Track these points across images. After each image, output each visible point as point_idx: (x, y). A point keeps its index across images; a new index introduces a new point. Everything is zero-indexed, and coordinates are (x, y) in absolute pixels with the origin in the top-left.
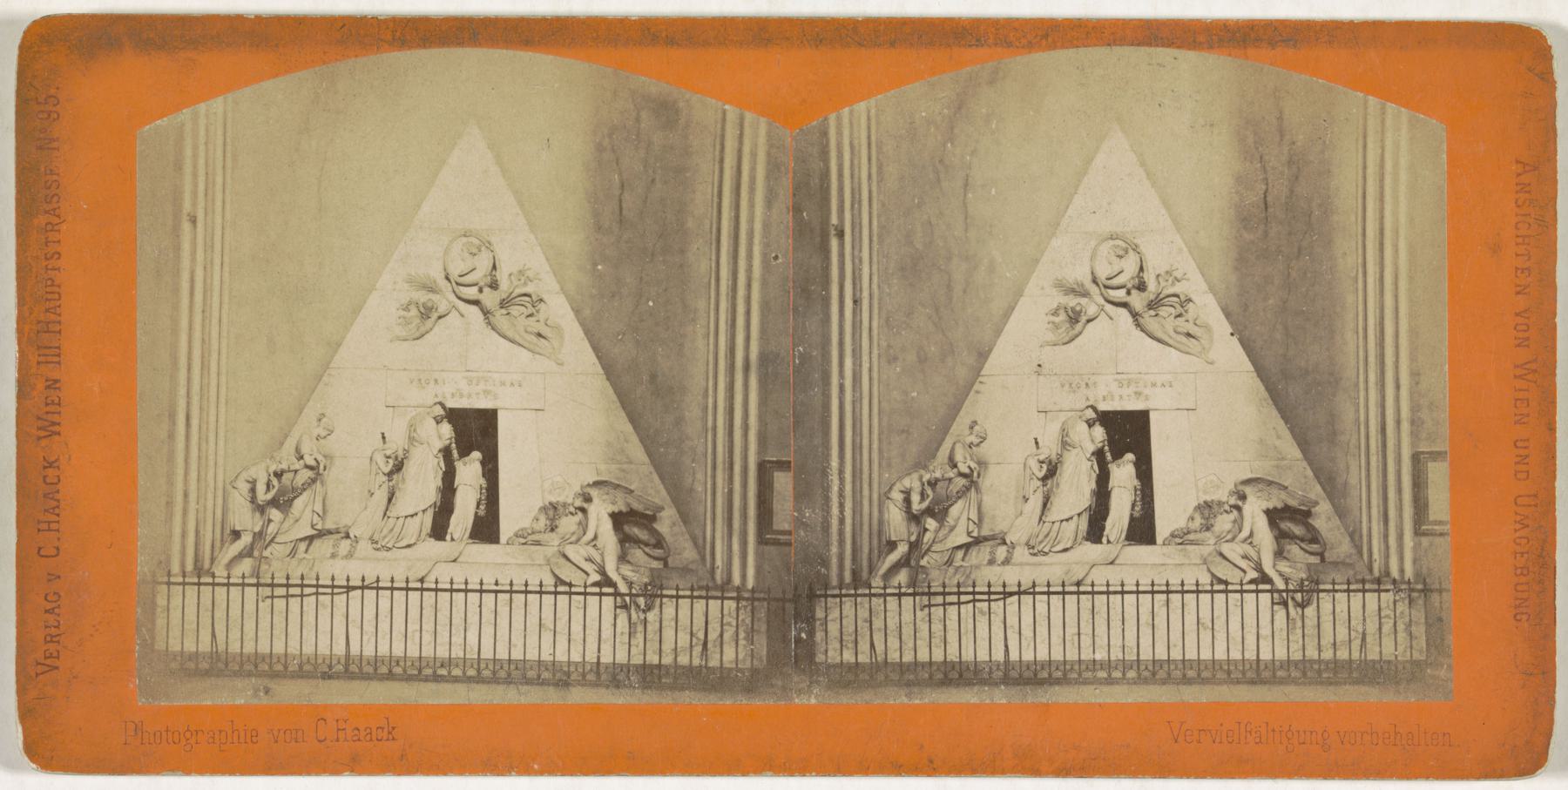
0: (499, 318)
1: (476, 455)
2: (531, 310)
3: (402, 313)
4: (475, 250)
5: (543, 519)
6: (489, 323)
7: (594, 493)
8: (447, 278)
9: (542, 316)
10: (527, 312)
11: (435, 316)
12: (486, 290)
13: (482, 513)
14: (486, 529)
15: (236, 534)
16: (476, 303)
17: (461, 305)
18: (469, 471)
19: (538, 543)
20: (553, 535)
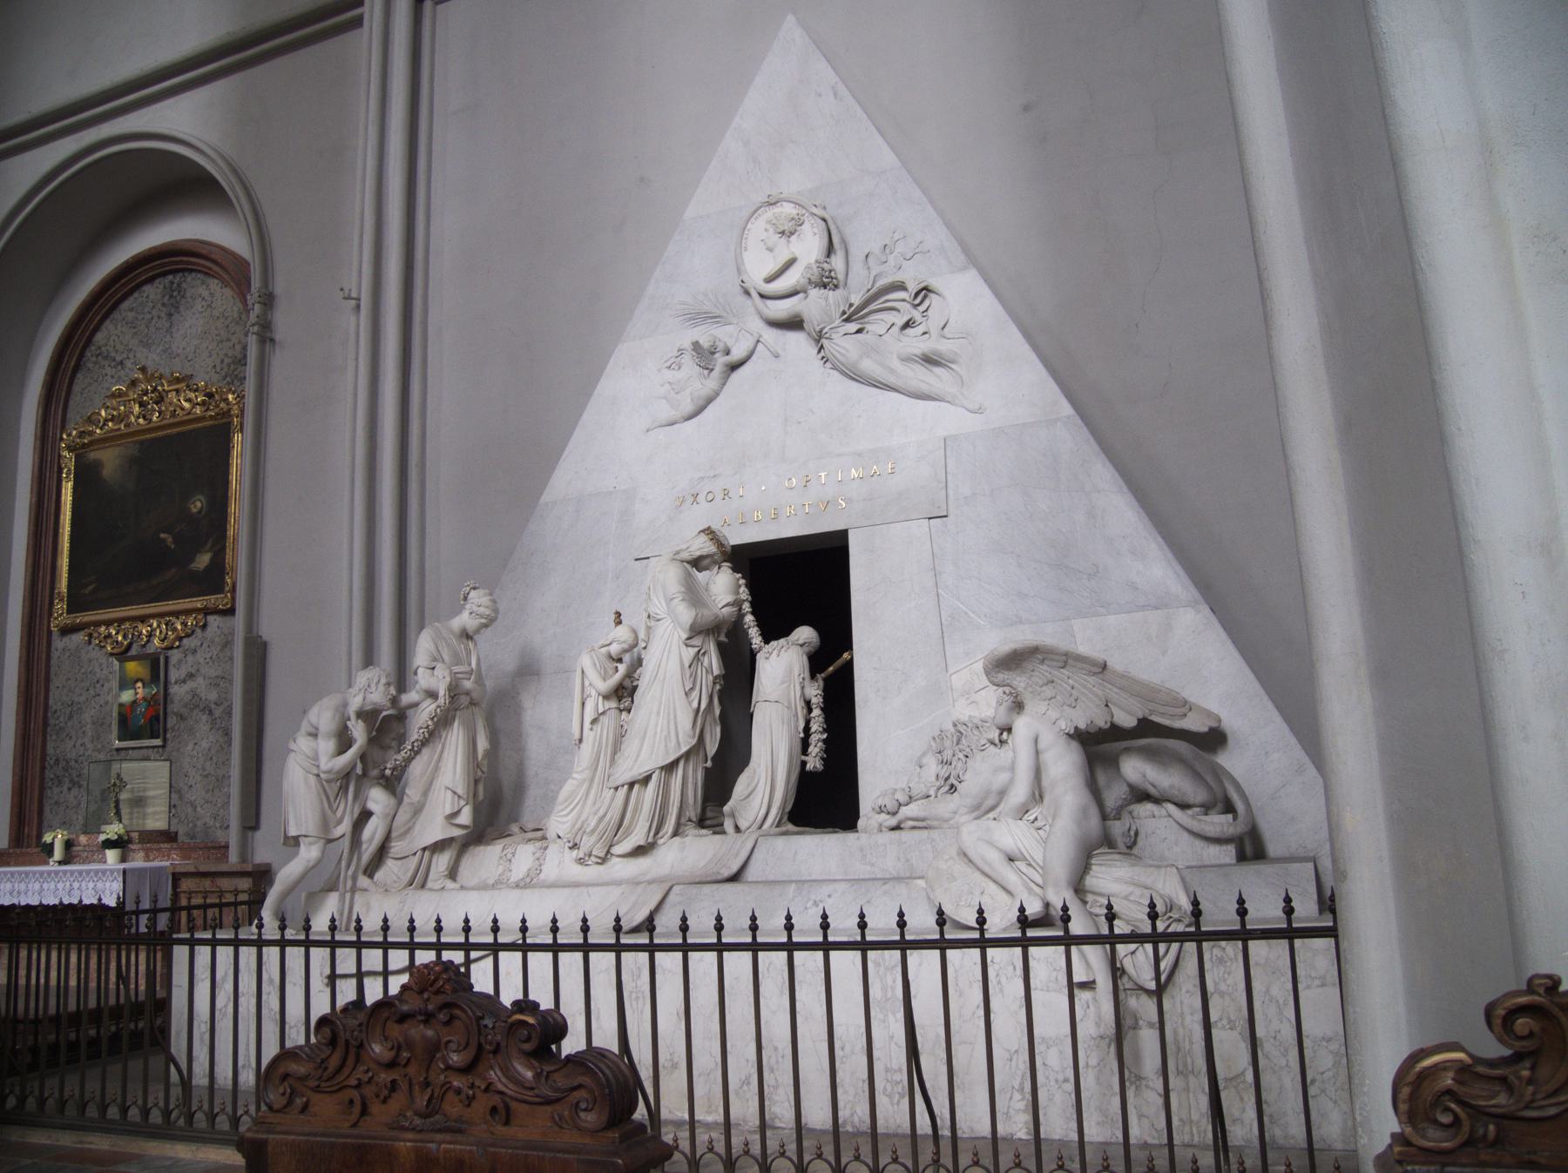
0: (844, 343)
1: (805, 634)
2: (907, 312)
3: (670, 375)
4: (787, 227)
5: (932, 767)
6: (825, 360)
7: (1019, 681)
8: (747, 293)
9: (934, 322)
10: (901, 321)
11: (721, 361)
12: (814, 293)
13: (814, 762)
14: (826, 798)
15: (294, 842)
16: (794, 324)
17: (771, 335)
18: (782, 668)
19: (921, 824)
20: (954, 802)
